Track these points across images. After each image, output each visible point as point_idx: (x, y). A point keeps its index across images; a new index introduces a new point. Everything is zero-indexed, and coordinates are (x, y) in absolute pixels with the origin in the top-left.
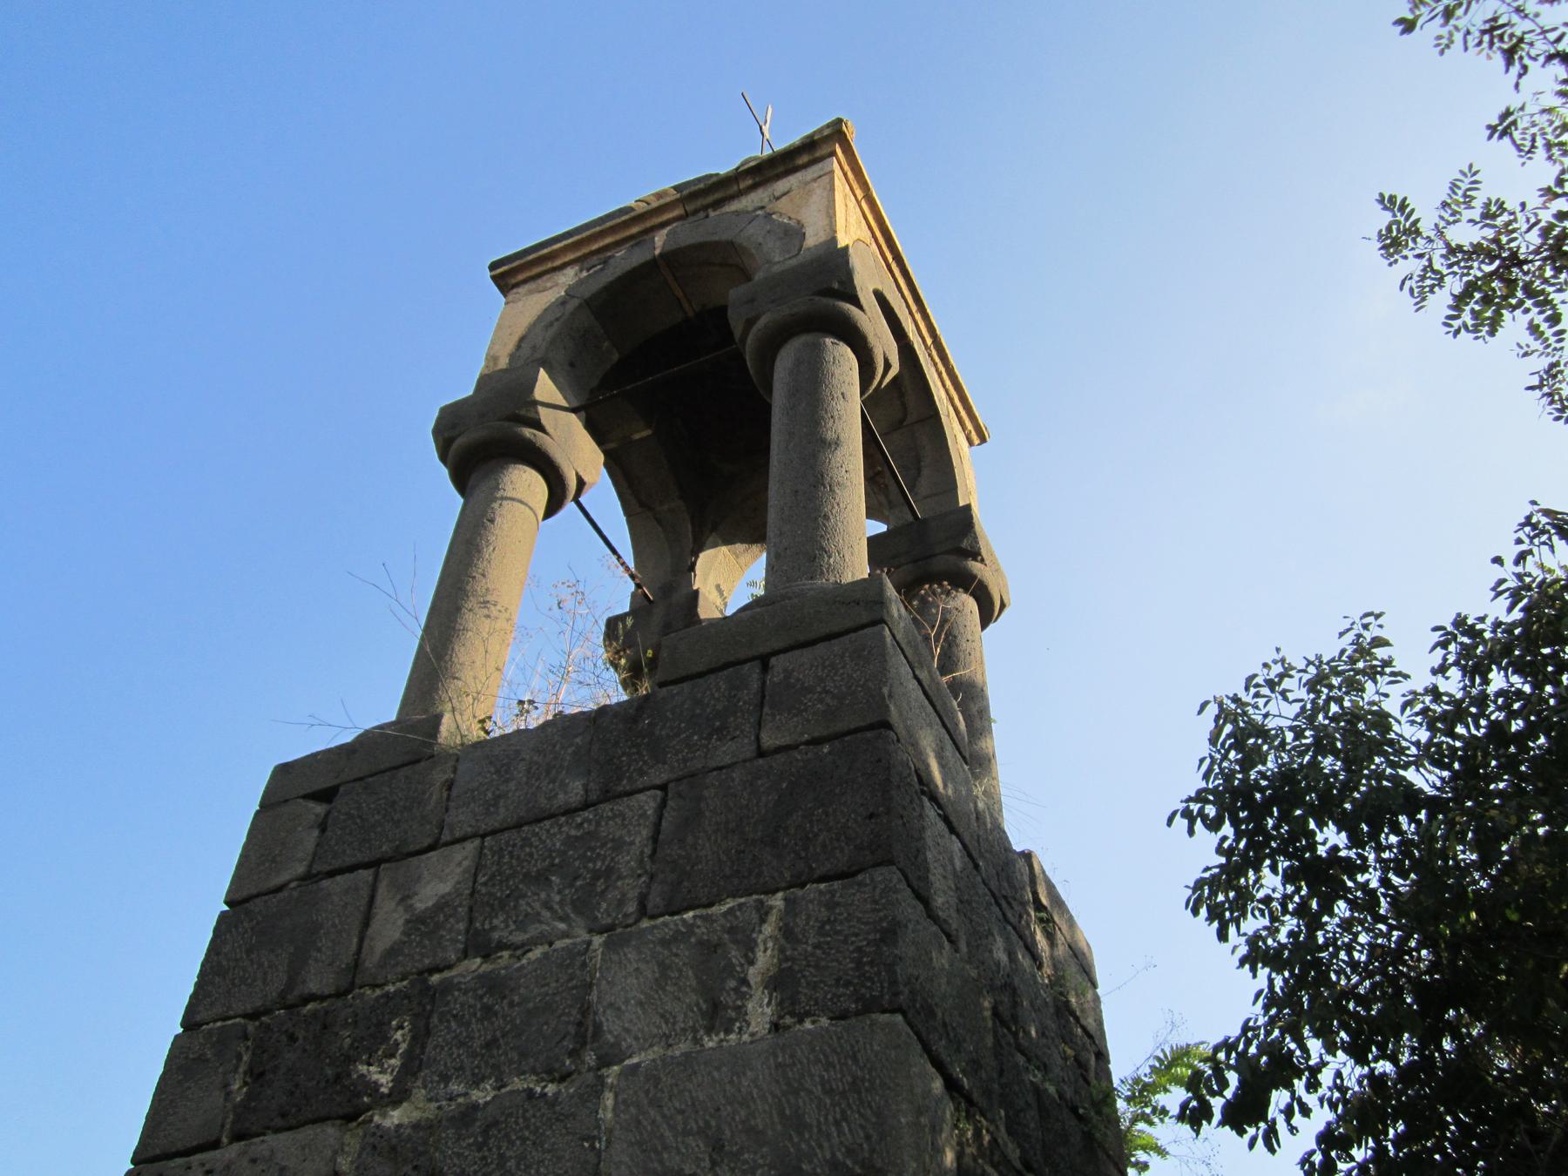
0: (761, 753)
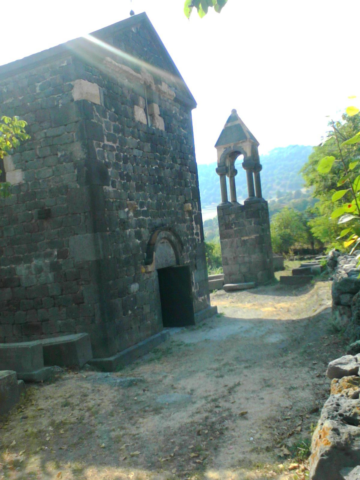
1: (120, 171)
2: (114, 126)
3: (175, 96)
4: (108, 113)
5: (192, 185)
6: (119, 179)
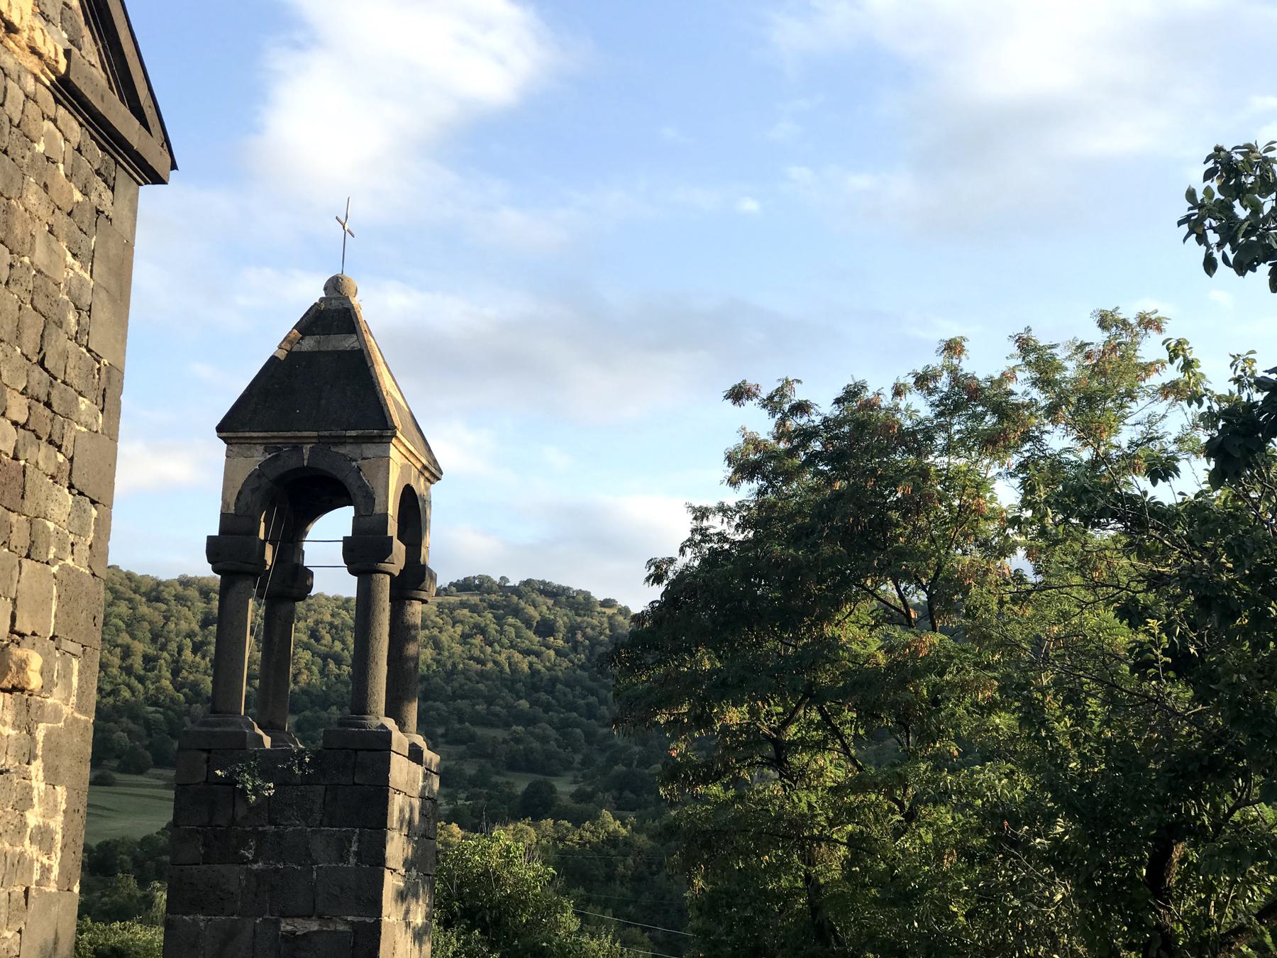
0: (355, 784)
3: (62, 68)
5: (69, 561)
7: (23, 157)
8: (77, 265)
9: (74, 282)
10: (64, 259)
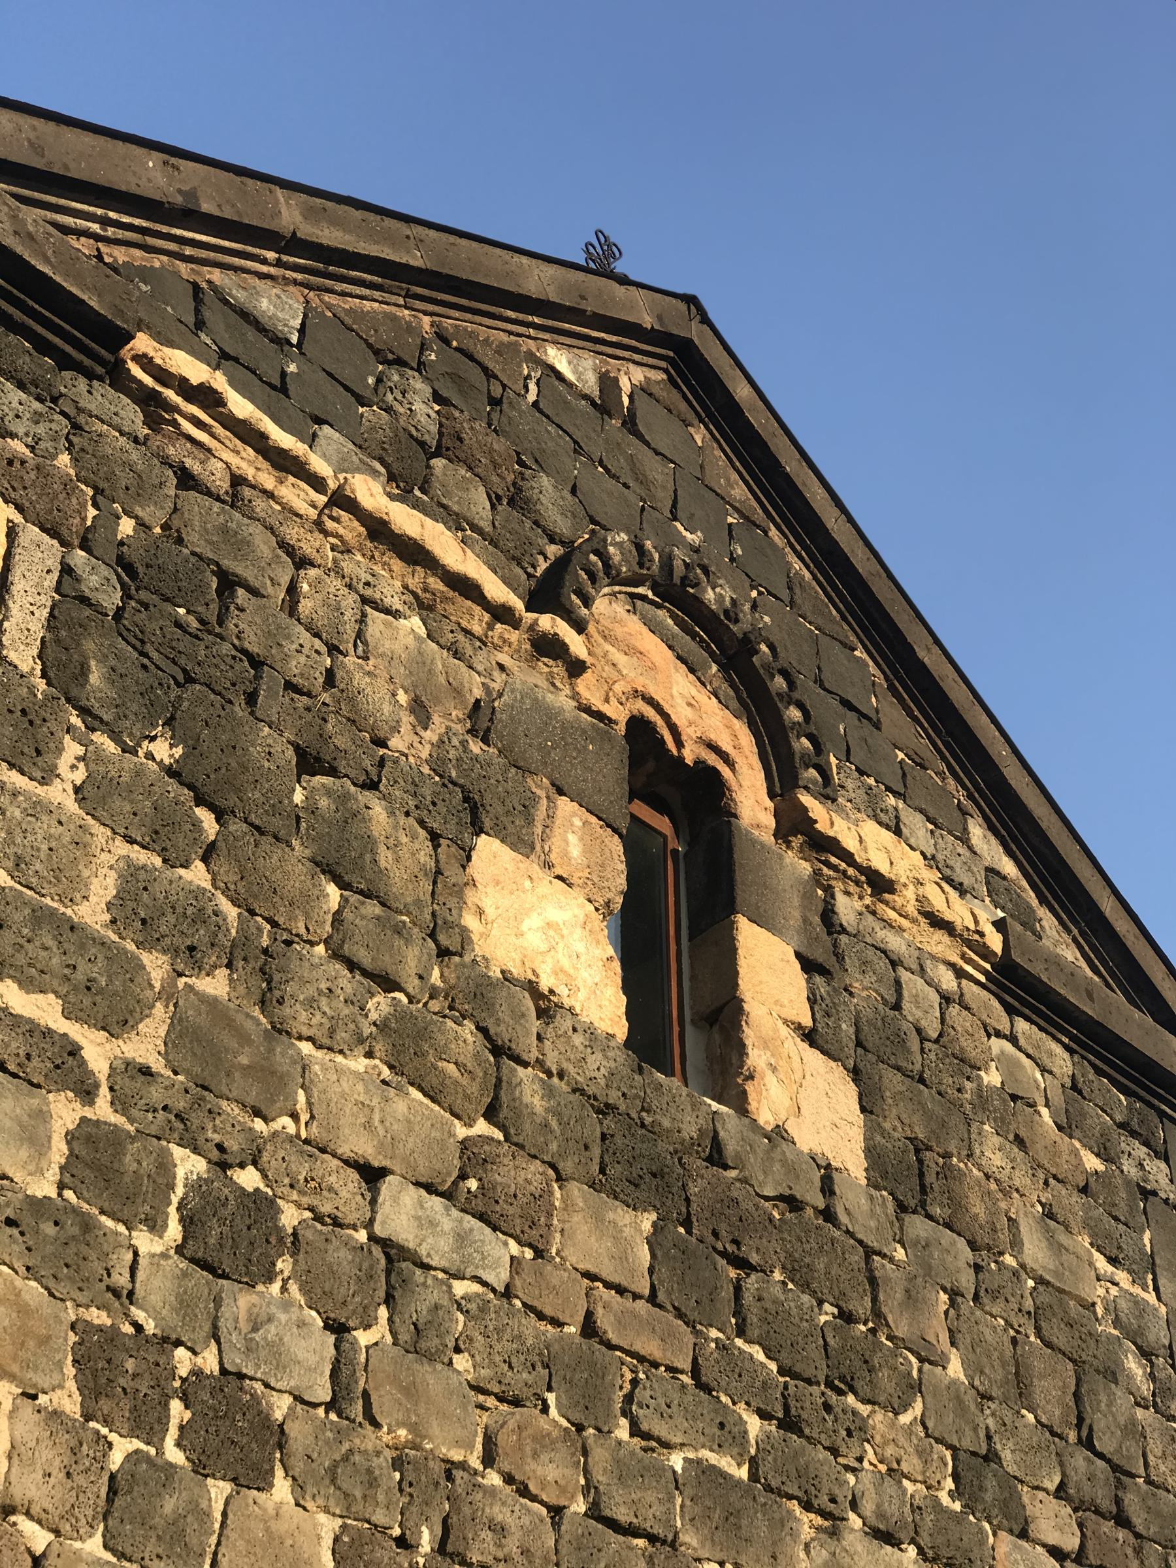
1: (98, 1317)
2: (131, 874)
4: (73, 749)
6: (69, 1401)
7: (959, 1090)
8: (1122, 1277)
9: (1123, 1304)
10: (1091, 1264)
